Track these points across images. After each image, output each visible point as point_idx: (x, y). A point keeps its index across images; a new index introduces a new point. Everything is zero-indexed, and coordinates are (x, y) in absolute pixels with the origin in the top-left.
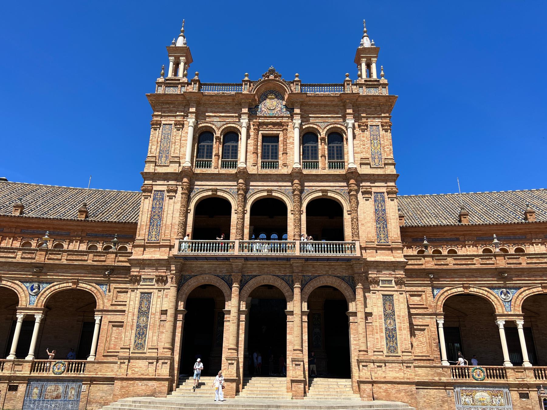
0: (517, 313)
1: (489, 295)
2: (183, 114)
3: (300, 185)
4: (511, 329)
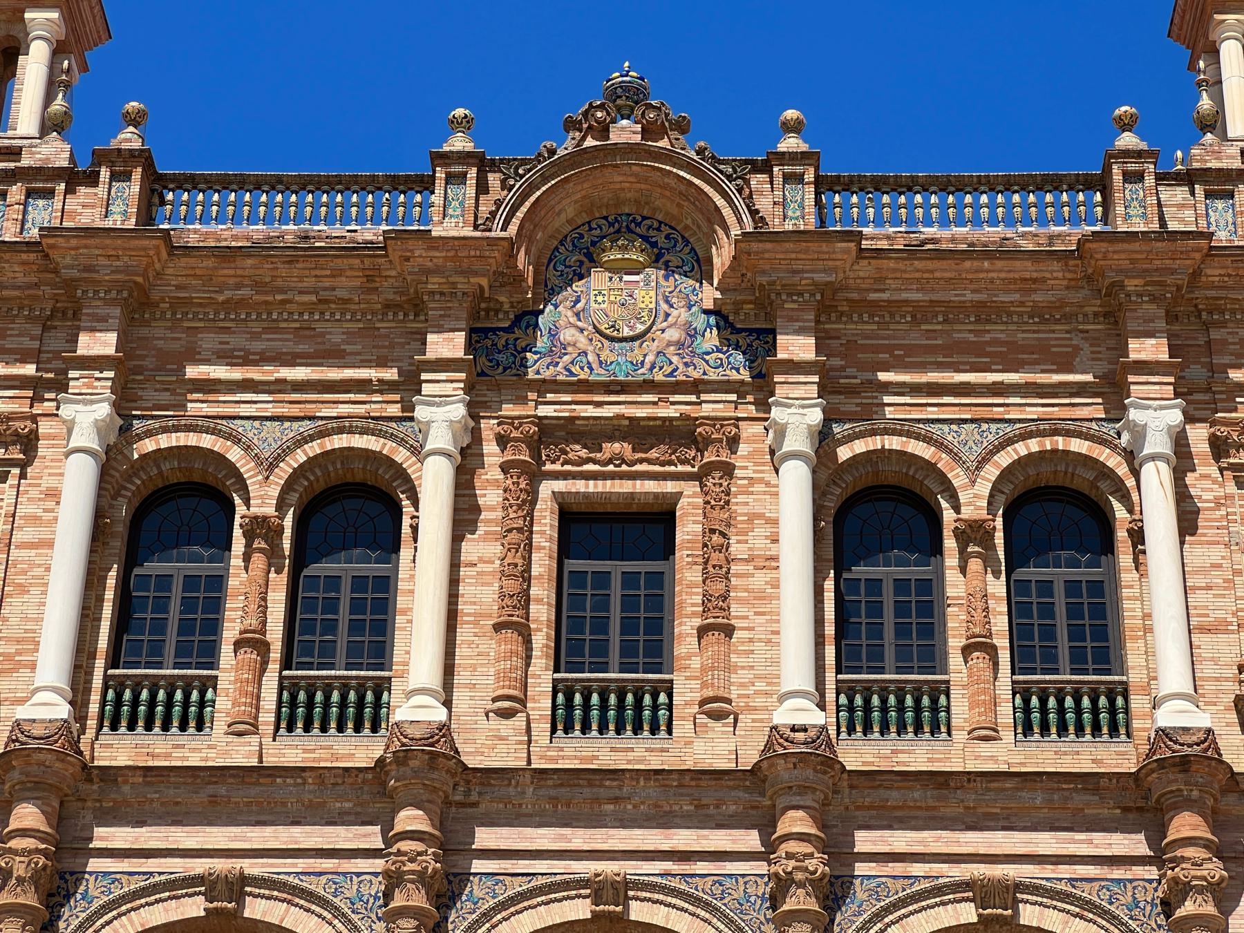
2: (30, 369)
3: (824, 846)
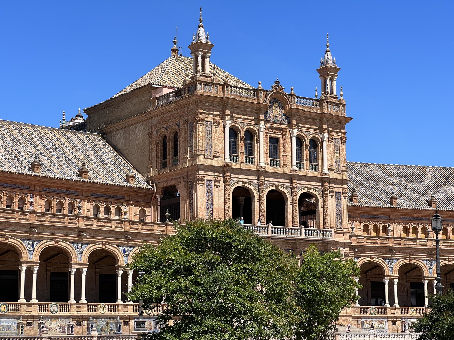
0: (395, 275)
2: (218, 113)
4: (391, 283)
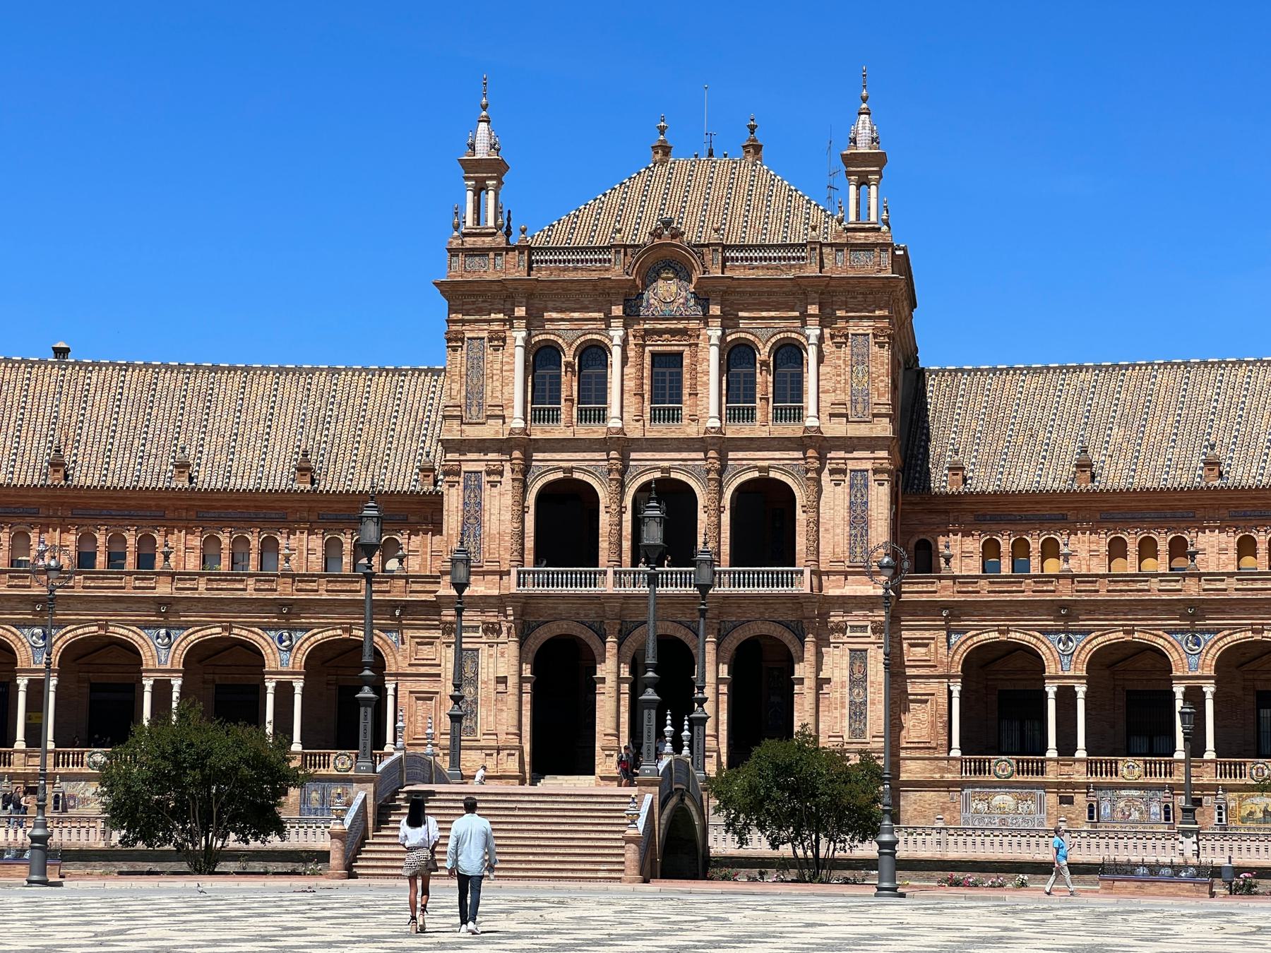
0: (1079, 673)
1: (1039, 644)
2: (501, 316)
3: (720, 460)
4: (1067, 696)
